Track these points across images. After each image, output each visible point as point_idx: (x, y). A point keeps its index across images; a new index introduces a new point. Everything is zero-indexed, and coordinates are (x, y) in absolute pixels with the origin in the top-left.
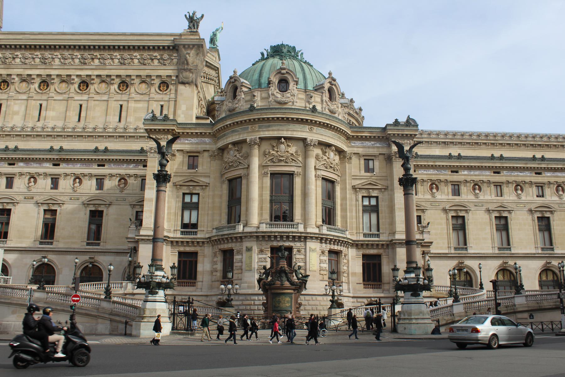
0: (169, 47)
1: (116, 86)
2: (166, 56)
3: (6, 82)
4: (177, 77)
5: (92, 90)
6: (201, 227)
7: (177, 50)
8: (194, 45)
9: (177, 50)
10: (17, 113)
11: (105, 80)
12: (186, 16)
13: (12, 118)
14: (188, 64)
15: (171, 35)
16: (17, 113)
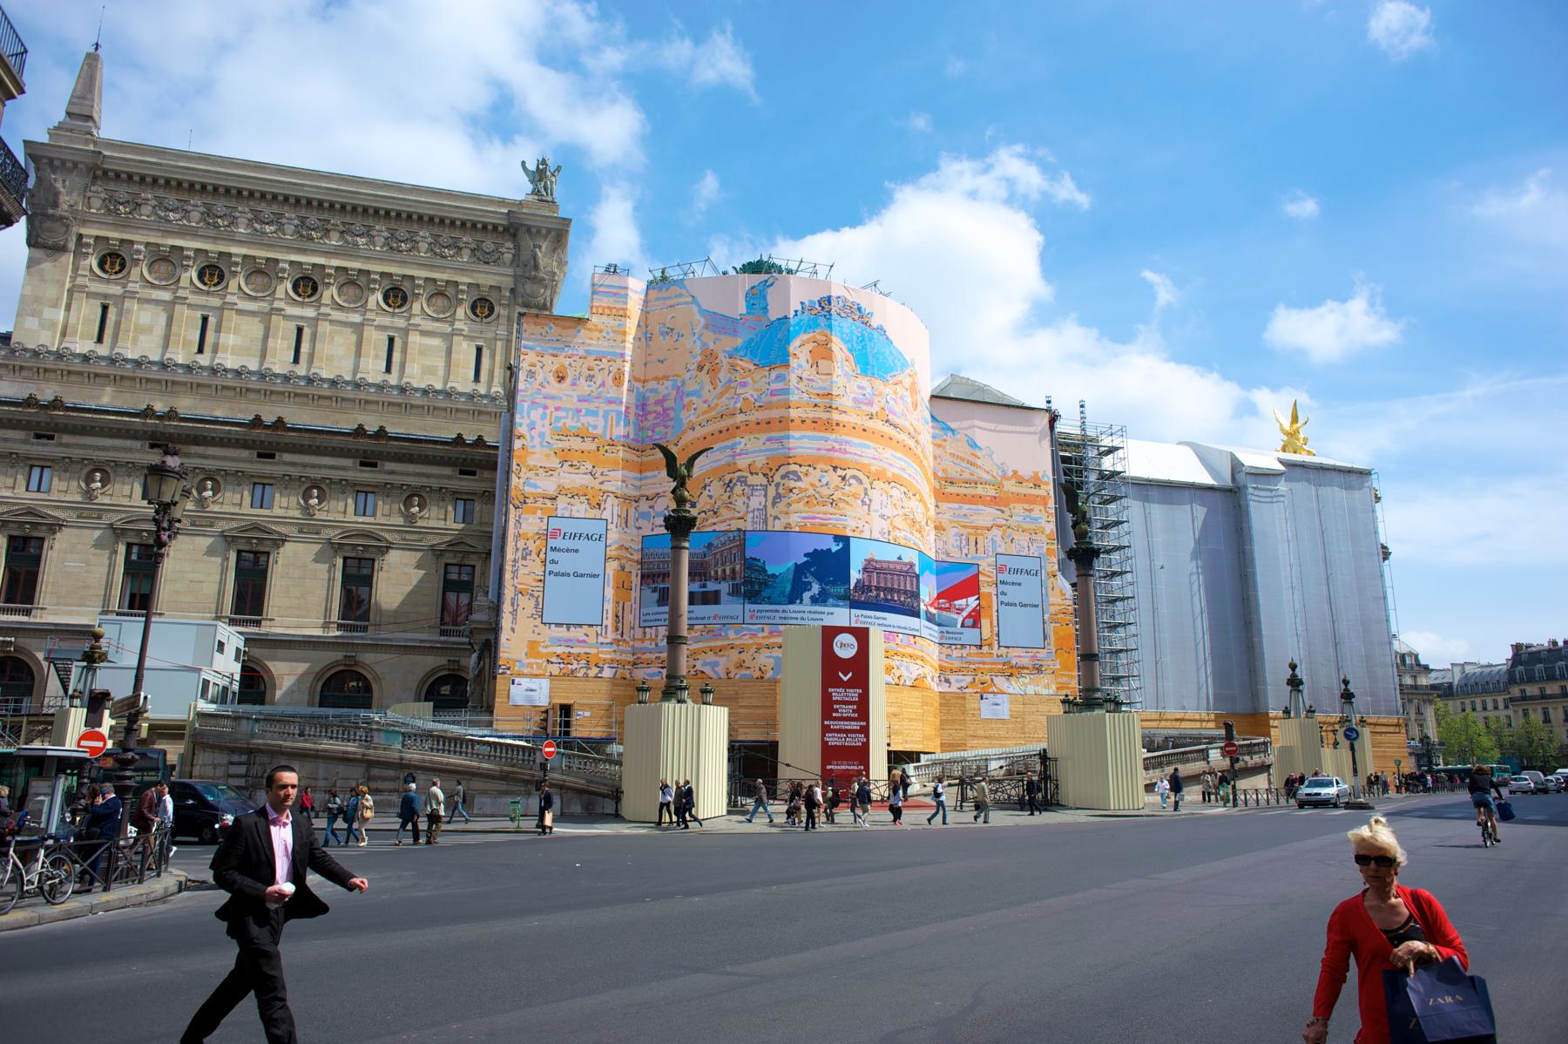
0: (495, 227)
1: (379, 296)
2: (488, 245)
3: (118, 256)
4: (512, 291)
5: (326, 299)
6: (890, 635)
7: (514, 236)
8: (549, 231)
9: (514, 236)
10: (148, 330)
11: (354, 283)
12: (523, 163)
13: (135, 340)
14: (536, 267)
15: (502, 202)
16: (148, 330)
